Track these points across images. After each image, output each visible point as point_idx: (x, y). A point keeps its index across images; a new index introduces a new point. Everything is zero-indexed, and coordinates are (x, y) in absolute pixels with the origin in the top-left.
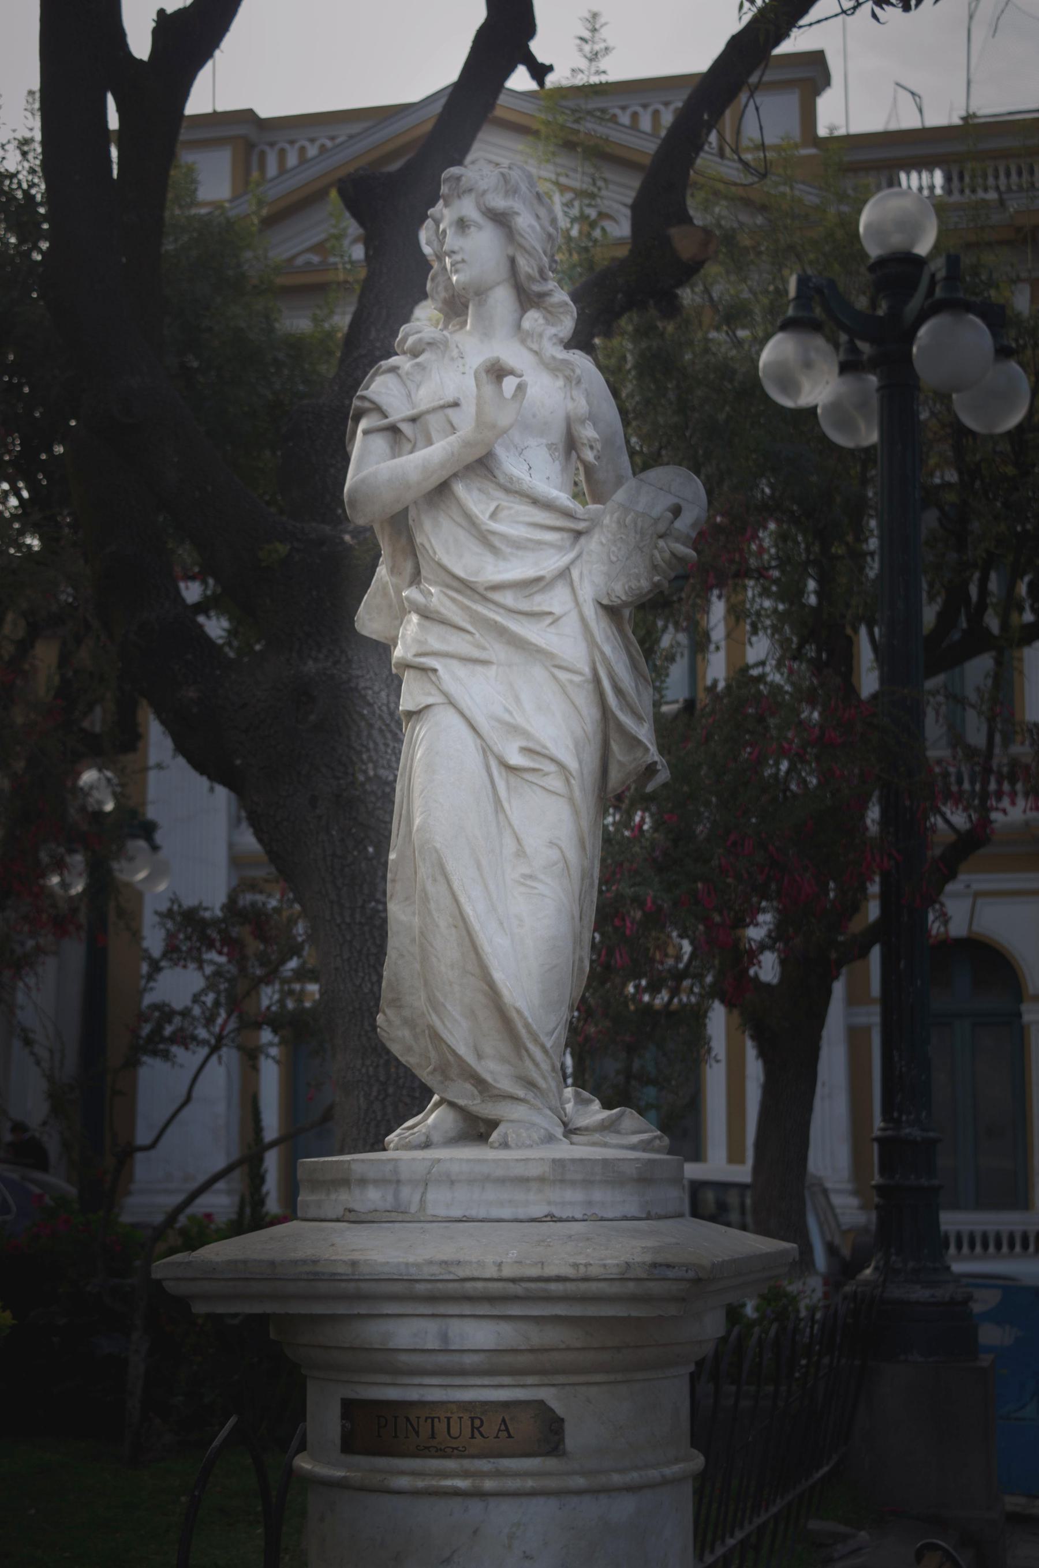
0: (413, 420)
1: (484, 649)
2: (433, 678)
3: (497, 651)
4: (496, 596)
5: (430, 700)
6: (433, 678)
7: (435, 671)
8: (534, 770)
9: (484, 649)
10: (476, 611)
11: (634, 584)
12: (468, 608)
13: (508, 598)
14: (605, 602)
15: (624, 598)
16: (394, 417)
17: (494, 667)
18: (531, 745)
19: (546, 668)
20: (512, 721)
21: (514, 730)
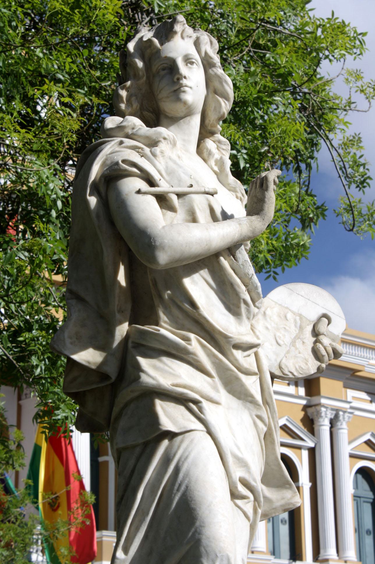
0: (180, 195)
1: (218, 391)
2: (194, 407)
3: (223, 395)
4: (235, 352)
5: (193, 428)
6: (194, 407)
7: (196, 402)
8: (243, 497)
9: (218, 391)
10: (220, 360)
11: (304, 366)
12: (215, 356)
13: (238, 354)
14: (277, 373)
15: (296, 374)
16: (164, 187)
17: (220, 407)
18: (246, 476)
19: (251, 416)
20: (240, 455)
21: (243, 463)
